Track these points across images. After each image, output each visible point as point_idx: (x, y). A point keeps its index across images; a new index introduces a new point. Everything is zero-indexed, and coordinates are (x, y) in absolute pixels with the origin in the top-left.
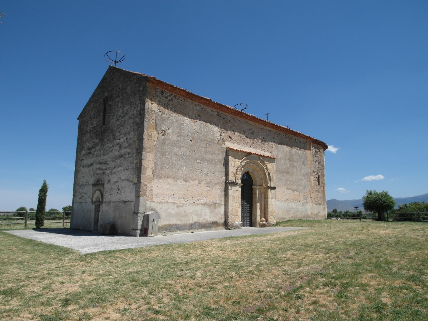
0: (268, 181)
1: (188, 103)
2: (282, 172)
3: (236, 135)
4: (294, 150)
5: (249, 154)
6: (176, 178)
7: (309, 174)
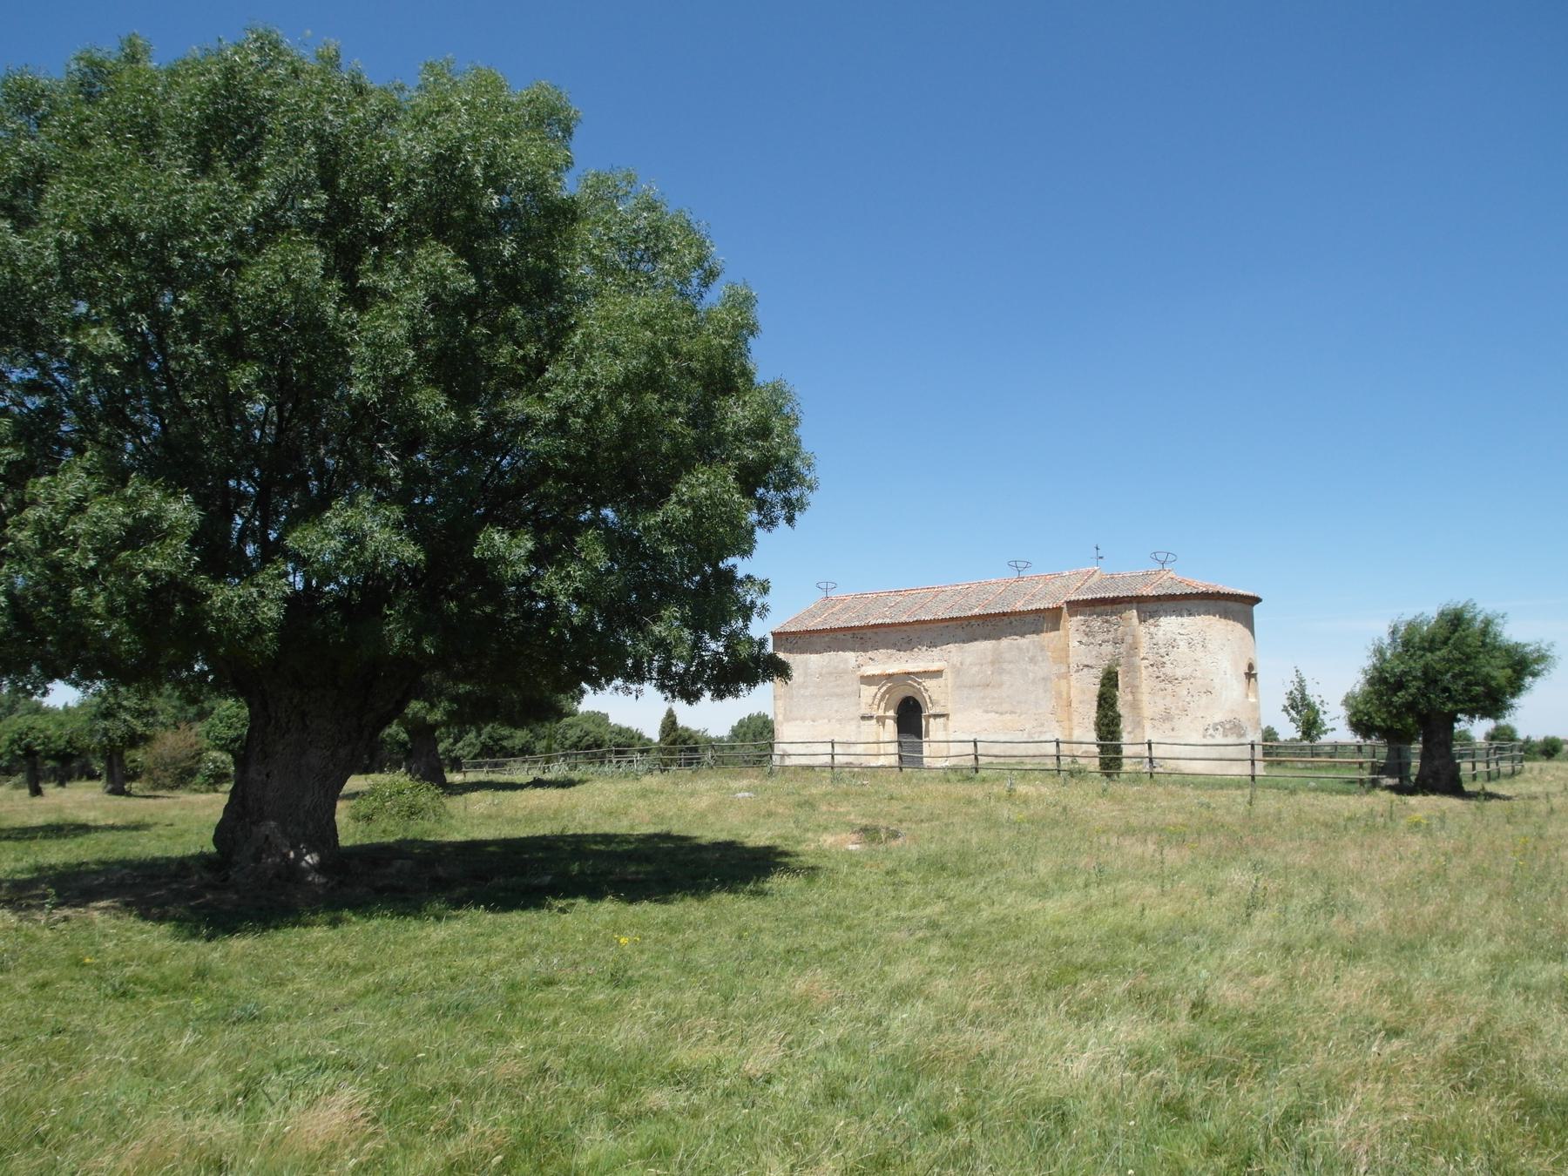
1: (815, 638)
2: (971, 687)
4: (1005, 642)
5: (890, 677)
6: (803, 719)
7: (1053, 677)
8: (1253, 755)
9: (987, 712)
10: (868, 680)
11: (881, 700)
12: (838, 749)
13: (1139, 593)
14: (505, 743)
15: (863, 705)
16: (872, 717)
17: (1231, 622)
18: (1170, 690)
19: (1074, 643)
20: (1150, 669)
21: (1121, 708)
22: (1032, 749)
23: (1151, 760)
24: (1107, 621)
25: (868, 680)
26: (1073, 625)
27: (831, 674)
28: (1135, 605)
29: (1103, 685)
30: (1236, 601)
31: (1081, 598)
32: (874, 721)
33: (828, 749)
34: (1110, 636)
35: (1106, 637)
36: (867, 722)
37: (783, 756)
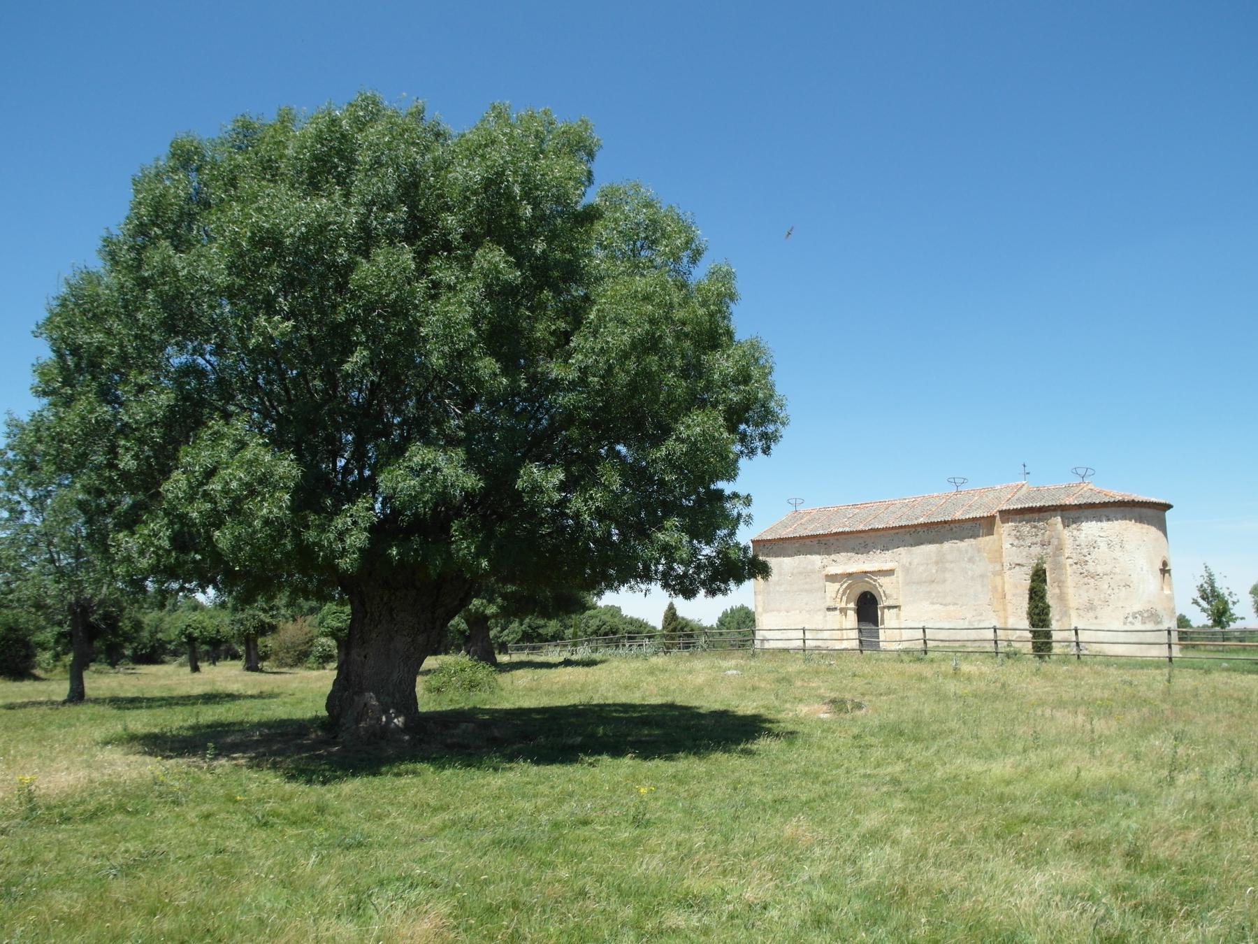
0: (884, 598)
3: (843, 556)
4: (947, 545)
5: (850, 575)
6: (779, 611)
7: (989, 574)
8: (1170, 639)
9: (933, 603)
10: (832, 578)
11: (843, 594)
12: (808, 635)
13: (1063, 503)
14: (541, 631)
15: (828, 599)
16: (836, 609)
17: (1146, 526)
18: (1092, 585)
19: (1006, 546)
20: (1074, 566)
21: (1050, 599)
22: (973, 635)
23: (1078, 644)
24: (1035, 527)
25: (832, 578)
26: (1005, 530)
27: (800, 573)
28: (1059, 513)
29: (1033, 581)
30: (1149, 507)
31: (1012, 507)
32: (838, 612)
33: (800, 634)
34: (1038, 539)
35: (1034, 540)
36: (832, 613)
37: (763, 640)
